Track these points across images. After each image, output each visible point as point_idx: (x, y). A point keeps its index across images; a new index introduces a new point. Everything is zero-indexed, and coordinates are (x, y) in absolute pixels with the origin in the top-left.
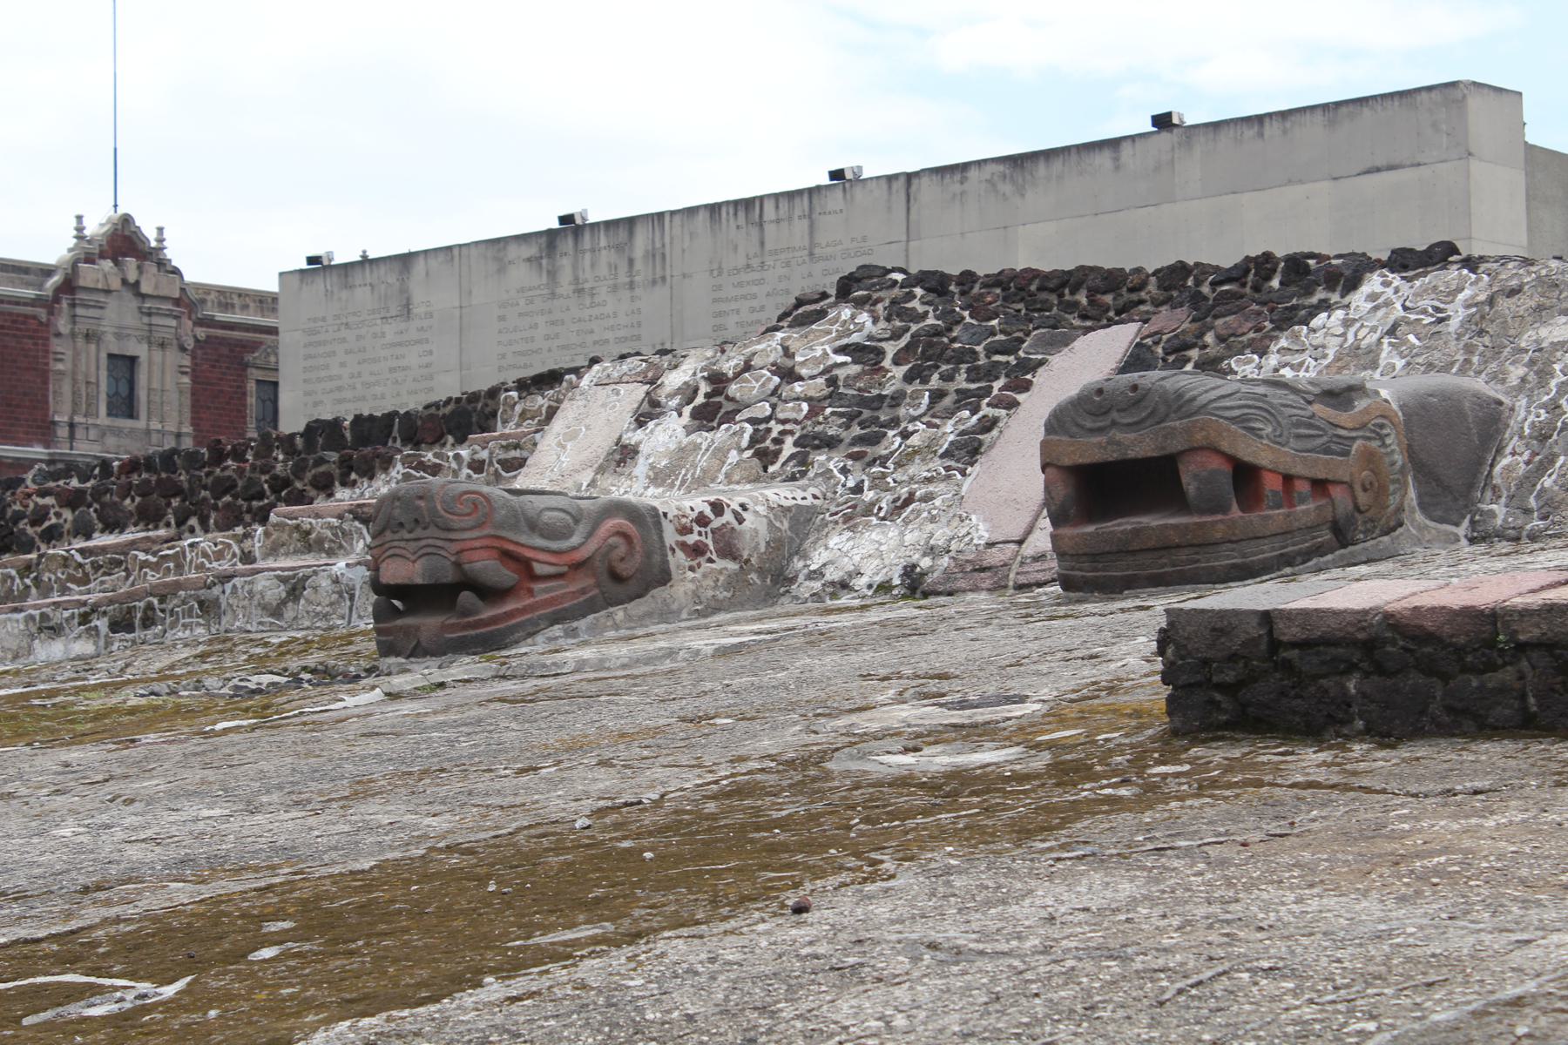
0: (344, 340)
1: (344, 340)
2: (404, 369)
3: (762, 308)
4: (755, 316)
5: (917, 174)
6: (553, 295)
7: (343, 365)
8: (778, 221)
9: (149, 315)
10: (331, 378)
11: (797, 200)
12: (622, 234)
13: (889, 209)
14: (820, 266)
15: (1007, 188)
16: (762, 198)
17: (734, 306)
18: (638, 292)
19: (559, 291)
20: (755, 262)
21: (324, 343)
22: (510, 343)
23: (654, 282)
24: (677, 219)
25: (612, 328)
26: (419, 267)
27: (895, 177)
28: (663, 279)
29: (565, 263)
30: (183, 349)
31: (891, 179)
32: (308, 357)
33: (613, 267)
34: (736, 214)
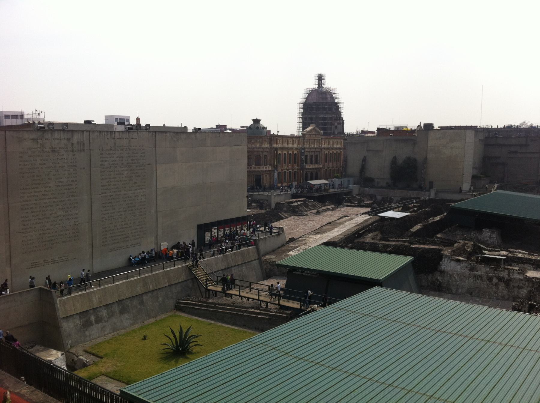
3: (115, 161)
4: (113, 163)
17: (107, 159)
18: (75, 153)
20: (113, 148)
23: (81, 151)
28: (84, 150)
34: (107, 135)
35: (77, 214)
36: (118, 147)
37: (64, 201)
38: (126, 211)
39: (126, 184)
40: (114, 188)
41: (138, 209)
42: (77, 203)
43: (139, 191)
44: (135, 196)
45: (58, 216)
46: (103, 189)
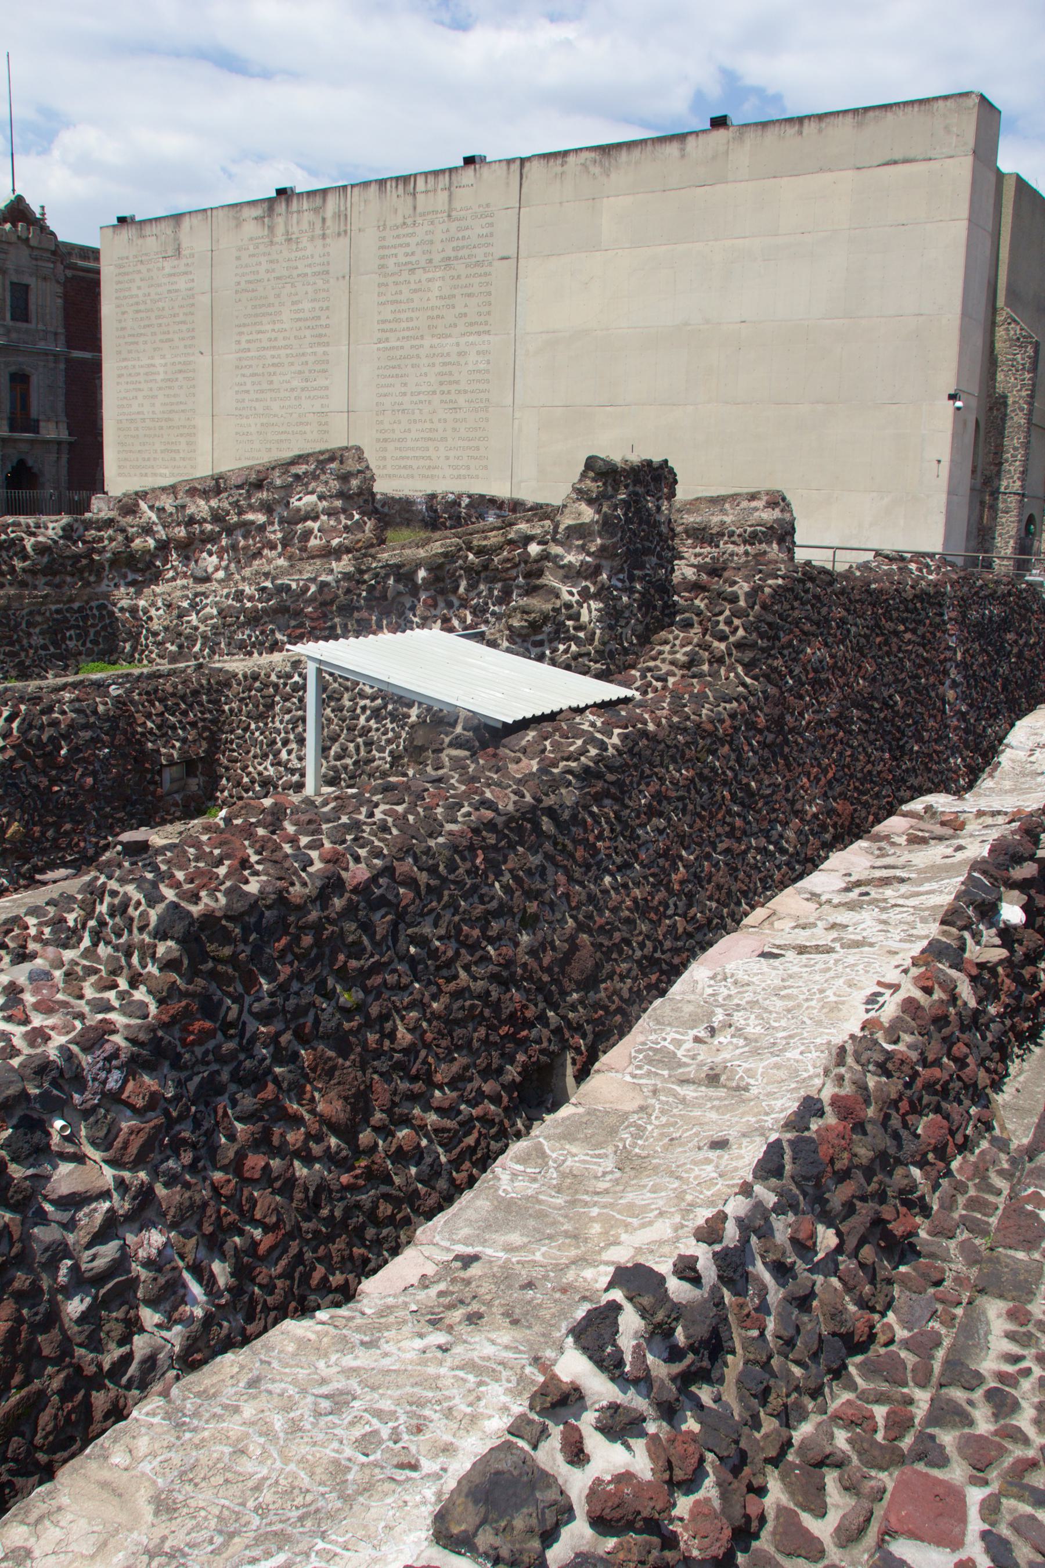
0: (139, 272)
1: (139, 272)
2: (177, 291)
3: (413, 254)
4: (408, 259)
5: (529, 159)
6: (272, 243)
7: (139, 288)
8: (427, 192)
9: (36, 260)
10: (132, 297)
11: (441, 177)
12: (318, 201)
13: (508, 184)
14: (454, 225)
15: (596, 170)
16: (415, 175)
17: (394, 251)
18: (328, 241)
19: (276, 240)
20: (409, 221)
21: (127, 274)
22: (243, 275)
23: (339, 235)
24: (356, 190)
25: (310, 266)
26: (186, 223)
27: (513, 160)
28: (345, 232)
29: (280, 221)
30: (58, 282)
31: (509, 162)
32: (119, 283)
33: (312, 224)
35: (327, 388)
36: (422, 215)
37: (303, 354)
38: (434, 393)
39: (438, 317)
40: (408, 329)
41: (465, 392)
42: (328, 362)
43: (471, 339)
44: (459, 354)
45: (293, 390)
46: (383, 331)
